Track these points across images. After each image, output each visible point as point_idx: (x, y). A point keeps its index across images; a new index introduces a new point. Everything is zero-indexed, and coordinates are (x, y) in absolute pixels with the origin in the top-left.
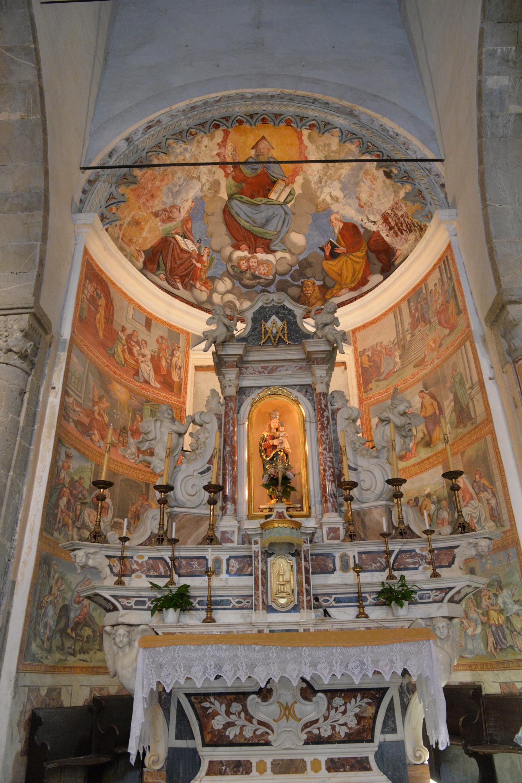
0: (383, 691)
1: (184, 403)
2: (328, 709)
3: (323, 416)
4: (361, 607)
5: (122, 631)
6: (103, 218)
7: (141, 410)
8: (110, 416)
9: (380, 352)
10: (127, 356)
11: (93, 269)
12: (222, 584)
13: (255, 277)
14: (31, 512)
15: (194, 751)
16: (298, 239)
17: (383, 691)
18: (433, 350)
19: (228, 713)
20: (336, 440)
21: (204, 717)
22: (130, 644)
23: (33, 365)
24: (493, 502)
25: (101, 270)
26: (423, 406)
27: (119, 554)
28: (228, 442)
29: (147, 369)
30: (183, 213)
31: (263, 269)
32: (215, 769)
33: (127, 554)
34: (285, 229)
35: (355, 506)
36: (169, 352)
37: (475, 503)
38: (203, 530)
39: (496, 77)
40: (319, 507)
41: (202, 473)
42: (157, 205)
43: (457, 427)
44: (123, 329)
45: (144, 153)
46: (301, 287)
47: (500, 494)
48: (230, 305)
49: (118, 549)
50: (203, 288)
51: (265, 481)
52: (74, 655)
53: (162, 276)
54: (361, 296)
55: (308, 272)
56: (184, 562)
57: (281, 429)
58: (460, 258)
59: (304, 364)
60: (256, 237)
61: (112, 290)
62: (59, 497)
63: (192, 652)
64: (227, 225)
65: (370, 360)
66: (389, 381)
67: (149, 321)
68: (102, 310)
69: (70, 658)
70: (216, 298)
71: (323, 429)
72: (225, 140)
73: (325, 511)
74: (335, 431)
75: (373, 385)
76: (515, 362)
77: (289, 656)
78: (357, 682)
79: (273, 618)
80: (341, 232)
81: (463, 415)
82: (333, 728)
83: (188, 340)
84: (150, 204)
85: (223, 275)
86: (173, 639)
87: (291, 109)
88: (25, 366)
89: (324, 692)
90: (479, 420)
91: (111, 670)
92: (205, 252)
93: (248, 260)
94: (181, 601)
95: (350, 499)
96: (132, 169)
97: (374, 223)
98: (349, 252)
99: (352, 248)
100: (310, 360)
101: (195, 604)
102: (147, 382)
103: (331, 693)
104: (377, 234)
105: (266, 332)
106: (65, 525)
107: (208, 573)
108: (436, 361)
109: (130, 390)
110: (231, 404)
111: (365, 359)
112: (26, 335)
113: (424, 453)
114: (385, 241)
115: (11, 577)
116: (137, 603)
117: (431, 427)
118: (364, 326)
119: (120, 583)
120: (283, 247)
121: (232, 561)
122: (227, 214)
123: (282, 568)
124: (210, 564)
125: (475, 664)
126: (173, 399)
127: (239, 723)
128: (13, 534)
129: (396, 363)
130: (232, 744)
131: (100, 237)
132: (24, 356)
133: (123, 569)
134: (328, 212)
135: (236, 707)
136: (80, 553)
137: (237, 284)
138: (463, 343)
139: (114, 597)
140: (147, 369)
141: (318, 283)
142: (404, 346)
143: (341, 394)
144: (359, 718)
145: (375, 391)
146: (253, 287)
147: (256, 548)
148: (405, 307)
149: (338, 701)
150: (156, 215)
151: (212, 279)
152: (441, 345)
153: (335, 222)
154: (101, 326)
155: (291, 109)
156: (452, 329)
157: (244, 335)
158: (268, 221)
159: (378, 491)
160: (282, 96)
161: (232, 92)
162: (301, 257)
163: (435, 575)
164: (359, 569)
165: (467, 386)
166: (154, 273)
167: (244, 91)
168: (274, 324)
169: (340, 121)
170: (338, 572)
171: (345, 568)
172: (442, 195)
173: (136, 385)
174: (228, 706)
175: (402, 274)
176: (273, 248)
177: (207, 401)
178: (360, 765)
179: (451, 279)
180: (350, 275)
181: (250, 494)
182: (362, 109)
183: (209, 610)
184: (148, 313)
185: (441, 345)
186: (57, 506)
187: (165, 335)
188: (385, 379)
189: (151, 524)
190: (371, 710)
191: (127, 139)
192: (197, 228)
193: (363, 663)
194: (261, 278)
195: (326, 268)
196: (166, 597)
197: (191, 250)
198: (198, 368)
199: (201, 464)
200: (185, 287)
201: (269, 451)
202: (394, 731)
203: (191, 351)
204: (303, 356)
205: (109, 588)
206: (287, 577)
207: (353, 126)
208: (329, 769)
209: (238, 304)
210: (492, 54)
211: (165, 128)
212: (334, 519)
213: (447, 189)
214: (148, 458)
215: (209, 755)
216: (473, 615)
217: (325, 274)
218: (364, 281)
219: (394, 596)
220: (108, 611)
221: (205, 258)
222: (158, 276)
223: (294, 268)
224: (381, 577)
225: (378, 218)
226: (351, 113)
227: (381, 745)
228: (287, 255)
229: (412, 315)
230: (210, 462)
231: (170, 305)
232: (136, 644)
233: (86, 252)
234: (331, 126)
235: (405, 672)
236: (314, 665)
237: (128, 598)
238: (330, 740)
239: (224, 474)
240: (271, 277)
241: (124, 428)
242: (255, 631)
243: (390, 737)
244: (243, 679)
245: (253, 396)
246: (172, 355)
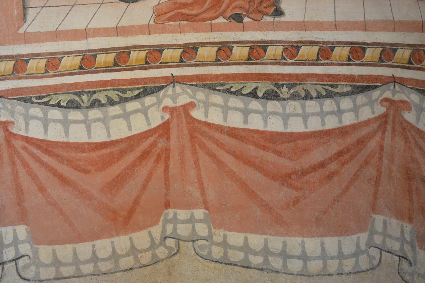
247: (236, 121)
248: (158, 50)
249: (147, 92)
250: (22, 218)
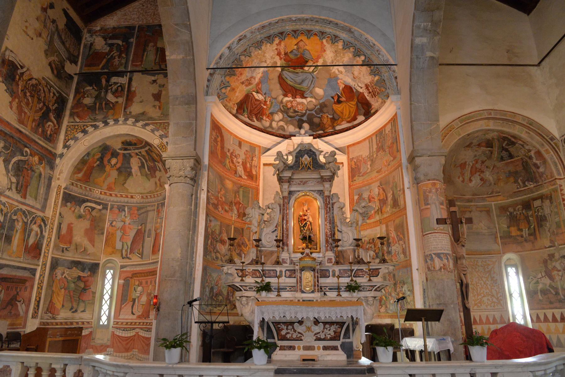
0: (344, 323)
1: (259, 185)
2: (324, 329)
3: (327, 207)
4: (339, 292)
5: (244, 299)
6: (219, 97)
7: (238, 192)
8: (225, 197)
9: (361, 161)
10: (231, 164)
11: (215, 123)
12: (283, 281)
13: (295, 111)
14: (199, 248)
15: (275, 343)
16: (319, 91)
17: (344, 323)
18: (385, 166)
19: (287, 329)
20: (333, 217)
21: (279, 331)
22: (247, 304)
23: (195, 181)
24: (404, 246)
25: (218, 122)
26: (379, 194)
27: (241, 268)
28: (284, 217)
29: (240, 169)
30: (257, 80)
31: (300, 107)
32: (282, 348)
33: (244, 268)
34: (312, 86)
35: (339, 248)
36: (250, 159)
37: (397, 245)
38: (274, 258)
39: (420, 38)
40: (324, 248)
41: (273, 232)
42: (243, 78)
43: (393, 208)
44: (229, 150)
45: (238, 57)
46: (321, 118)
47: (407, 243)
48: (282, 128)
49: (240, 266)
50: (267, 119)
51: (301, 237)
52: (216, 308)
53: (246, 115)
54: (354, 127)
55: (325, 110)
56: (267, 272)
57: (308, 211)
58: (401, 122)
59: (320, 180)
60: (296, 90)
61: (223, 131)
62: (208, 240)
63: (275, 308)
64: (280, 84)
65: (355, 165)
66: (365, 176)
67: (240, 142)
68: (219, 143)
69: (215, 309)
70: (274, 124)
71: (327, 213)
72: (280, 42)
73: (327, 250)
74: (333, 213)
75: (356, 178)
76: (418, 184)
77: (310, 310)
78: (334, 319)
79: (304, 295)
80: (343, 90)
81: (395, 203)
82: (325, 335)
83: (260, 151)
84: (239, 79)
85: (278, 111)
86: (264, 303)
87: (317, 28)
88: (192, 183)
89: (322, 323)
90: (402, 207)
91: (240, 314)
92: (268, 100)
93: (291, 102)
94: (267, 288)
95: (337, 246)
96: (233, 68)
97: (361, 88)
98: (347, 101)
99: (350, 99)
100: (323, 180)
101: (273, 289)
102: (240, 177)
103: (325, 323)
104: (362, 94)
105: (302, 164)
106: (211, 252)
107: (278, 277)
108: (387, 172)
109: (233, 182)
110: (286, 201)
111: (353, 163)
112: (192, 169)
114: (366, 99)
115: (193, 275)
116: (249, 288)
117: (382, 205)
118: (354, 145)
119: (242, 280)
120: (311, 95)
121: (287, 272)
122: (281, 80)
123: (308, 276)
124: (278, 274)
125: (393, 316)
126: (253, 184)
127: (291, 333)
128: (192, 258)
129: (368, 168)
130: (288, 340)
131: (217, 106)
132: (192, 179)
133: (243, 274)
134: (336, 78)
135: (290, 327)
136: (225, 268)
137: (286, 116)
138: (397, 168)
139: (241, 286)
140: (240, 169)
141: (330, 116)
142: (372, 160)
143: (336, 195)
144: (335, 332)
145: (357, 182)
146: (294, 117)
147: (297, 268)
148: (374, 137)
149: (327, 326)
150: (243, 83)
151: (272, 114)
152: (389, 165)
153: (340, 84)
154: (219, 152)
155: (317, 28)
156: (395, 158)
157: (291, 165)
158: (303, 81)
159: (350, 243)
160: (312, 19)
161: (284, 17)
162: (321, 102)
163: (370, 280)
164: (339, 277)
165: (398, 189)
166: (242, 115)
167: (291, 16)
168: (306, 159)
169: (343, 35)
170: (331, 277)
171: (334, 275)
172: (395, 84)
173: (235, 179)
174: (287, 327)
175: (373, 121)
176: (305, 96)
177: (275, 197)
178: (335, 348)
179: (395, 131)
180: (347, 114)
181: (294, 242)
182: (357, 29)
183: (279, 292)
184: (240, 138)
185: (389, 165)
186: (207, 244)
187: (248, 149)
188: (362, 176)
189: (252, 254)
190: (339, 330)
191: (229, 48)
192: (264, 87)
193: (336, 313)
194: (298, 112)
195: (334, 108)
196: (261, 287)
197: (261, 99)
198: (265, 165)
199: (272, 228)
200: (258, 120)
201: (302, 220)
202: (349, 338)
203: (261, 157)
204: (319, 177)
205: (238, 283)
206: (310, 279)
207: (350, 39)
208: (323, 349)
209: (286, 127)
210: (419, 27)
211: (249, 40)
212: (330, 254)
213: (398, 80)
214: (250, 226)
215: (280, 343)
216: (393, 295)
217: (334, 112)
218: (355, 119)
219: (351, 288)
220: (238, 291)
221: (268, 103)
222: (244, 116)
223: (317, 107)
224: (347, 280)
225: (363, 86)
226: (350, 31)
227: (342, 342)
228: (313, 100)
229: (377, 145)
230: (276, 227)
231: (251, 133)
232: (250, 304)
233: (212, 115)
234: (338, 39)
235: (352, 317)
236: (319, 313)
237: (246, 286)
238: (324, 340)
239: (283, 233)
240: (304, 112)
241: (231, 202)
242: (297, 301)
243: (347, 340)
244: (293, 317)
245: (295, 195)
246: (252, 160)
247: (143, 335)
248: (136, 323)
249: (134, 329)
250: (113, 347)
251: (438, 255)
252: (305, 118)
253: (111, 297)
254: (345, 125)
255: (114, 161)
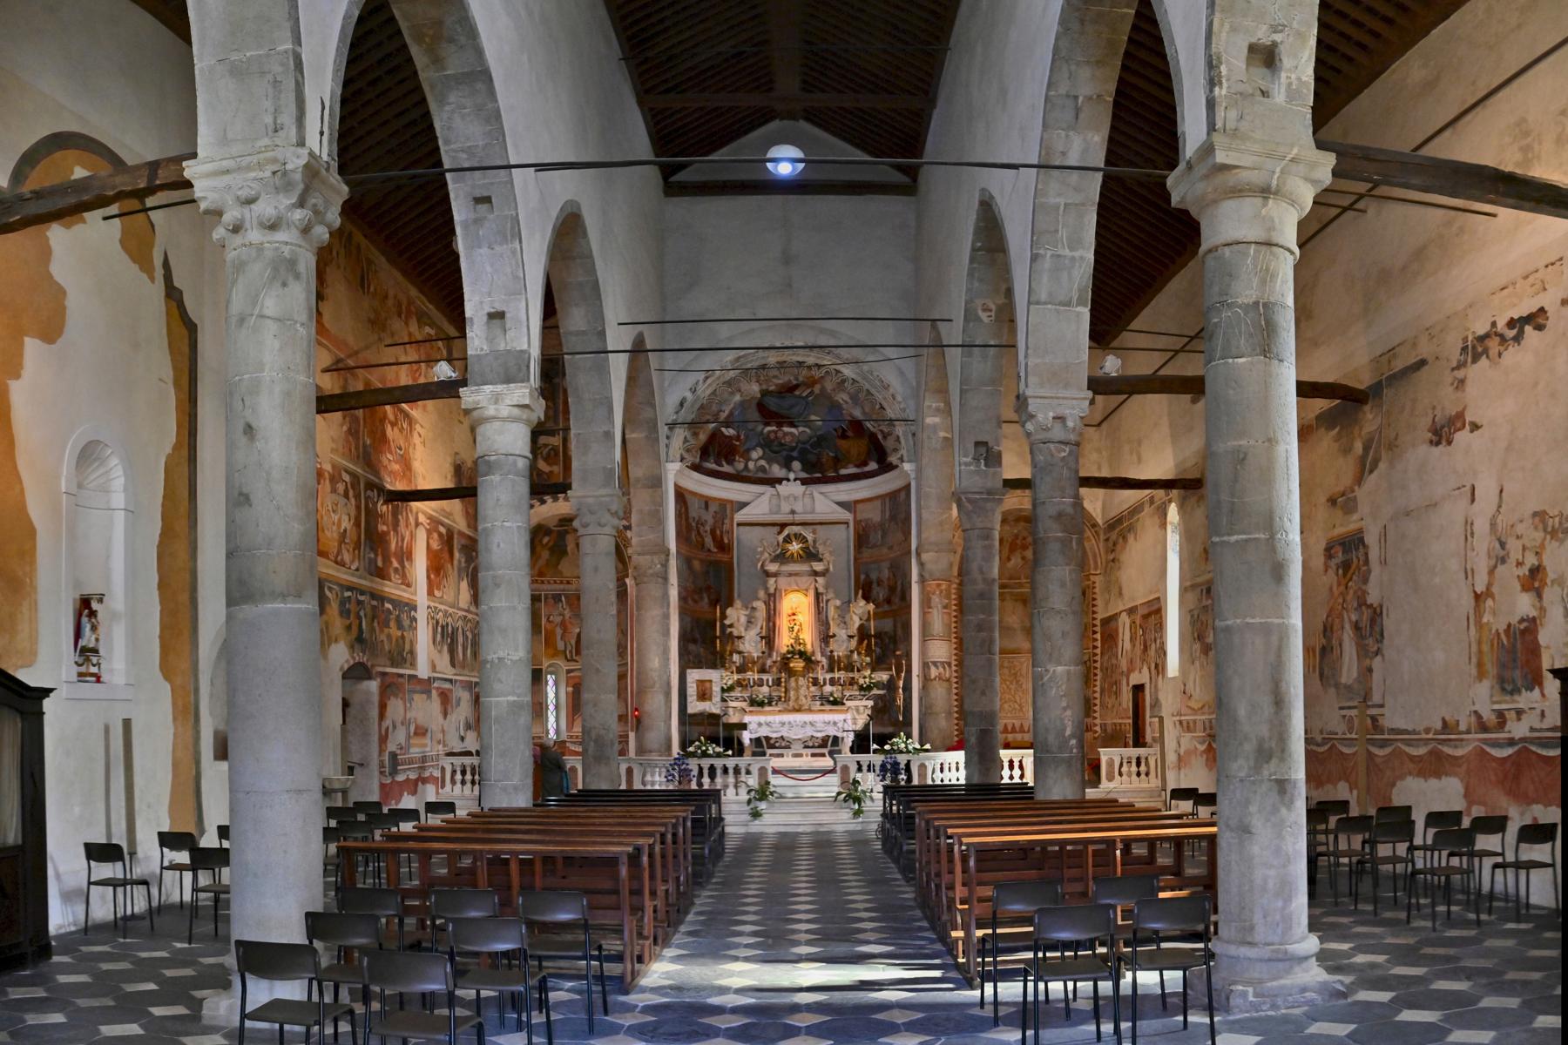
31: (788, 439)
48: (763, 469)
67: (707, 502)
70: (751, 465)
113: (886, 608)
126: (725, 557)
140: (709, 541)
151: (748, 451)
158: (792, 406)
218: (865, 464)
251: (935, 664)
252: (795, 454)
253: (557, 707)
254: (852, 470)
255: (546, 540)
